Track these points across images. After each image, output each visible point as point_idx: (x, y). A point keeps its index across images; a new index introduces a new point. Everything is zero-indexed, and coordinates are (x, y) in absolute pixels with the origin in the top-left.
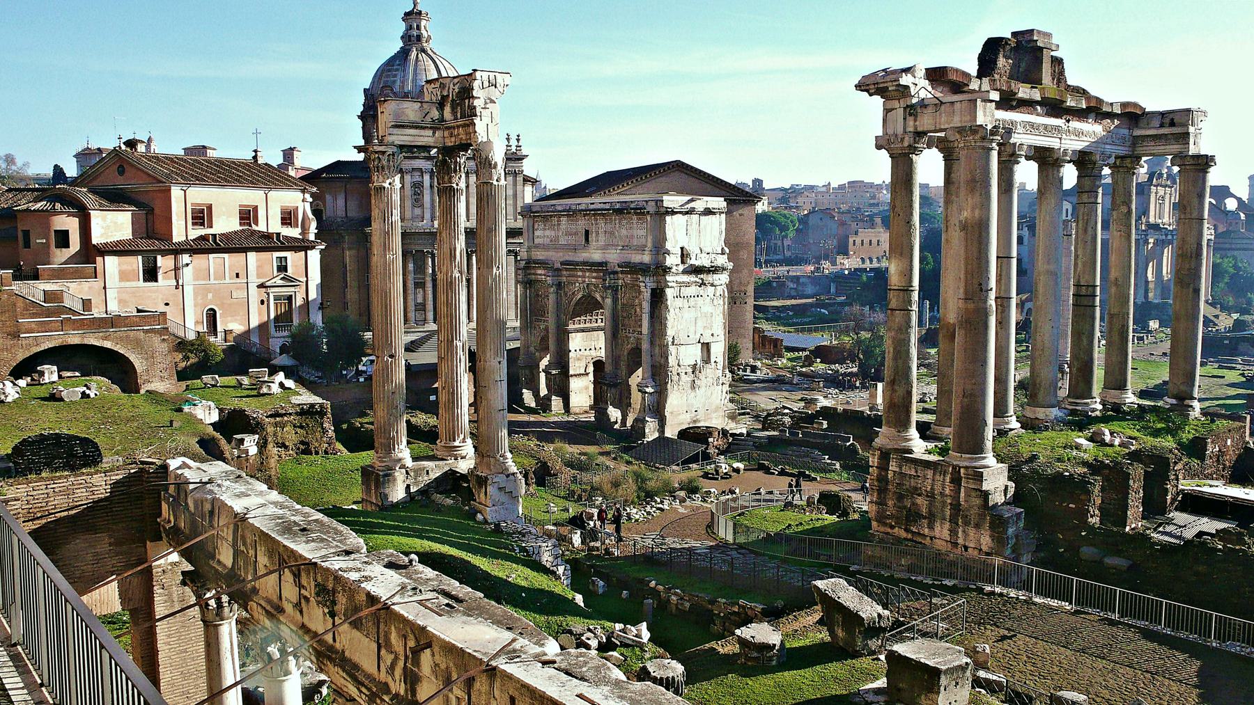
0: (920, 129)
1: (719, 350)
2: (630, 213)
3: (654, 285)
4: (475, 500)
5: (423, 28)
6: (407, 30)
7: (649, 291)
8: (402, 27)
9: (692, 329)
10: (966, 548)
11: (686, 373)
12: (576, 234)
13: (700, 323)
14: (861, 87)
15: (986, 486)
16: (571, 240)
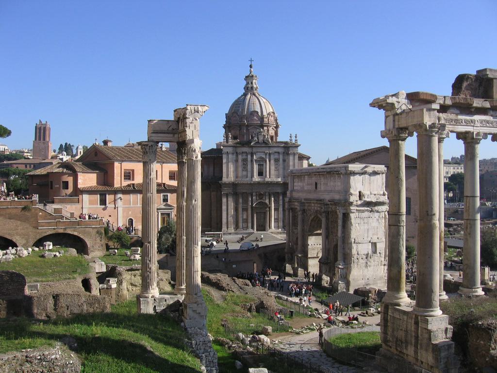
0: (401, 126)
1: (382, 246)
2: (334, 174)
3: (345, 211)
4: (184, 316)
5: (254, 83)
6: (246, 85)
7: (342, 214)
8: (245, 83)
9: (366, 235)
10: (422, 363)
11: (362, 258)
12: (311, 184)
13: (370, 233)
14: (372, 105)
15: (430, 327)
16: (309, 187)
